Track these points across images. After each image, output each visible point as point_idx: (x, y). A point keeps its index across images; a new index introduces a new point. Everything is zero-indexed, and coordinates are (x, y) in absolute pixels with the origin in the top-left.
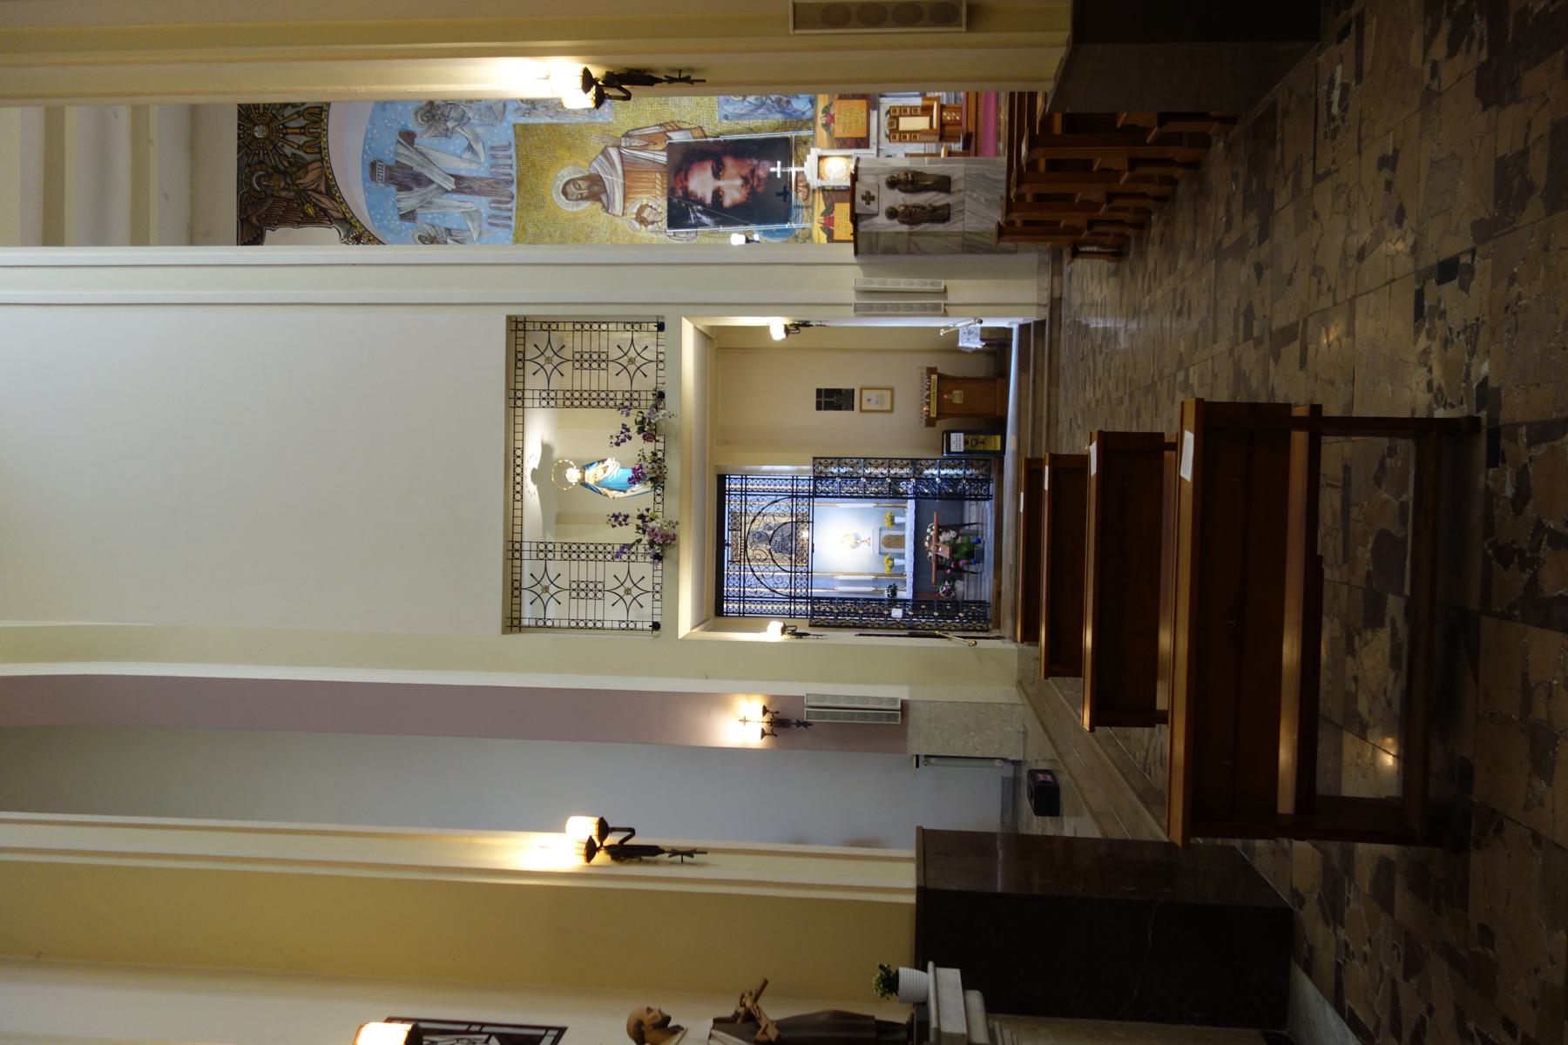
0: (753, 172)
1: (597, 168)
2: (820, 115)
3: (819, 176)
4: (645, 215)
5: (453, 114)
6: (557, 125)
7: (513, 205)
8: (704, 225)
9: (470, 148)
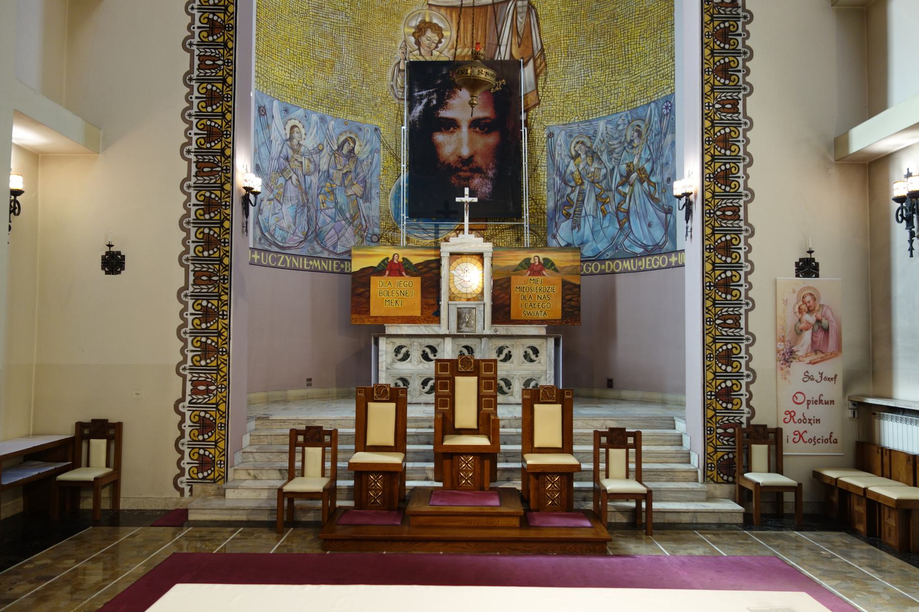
0: (478, 170)
2: (542, 256)
3: (454, 255)
4: (429, 33)
8: (411, 109)
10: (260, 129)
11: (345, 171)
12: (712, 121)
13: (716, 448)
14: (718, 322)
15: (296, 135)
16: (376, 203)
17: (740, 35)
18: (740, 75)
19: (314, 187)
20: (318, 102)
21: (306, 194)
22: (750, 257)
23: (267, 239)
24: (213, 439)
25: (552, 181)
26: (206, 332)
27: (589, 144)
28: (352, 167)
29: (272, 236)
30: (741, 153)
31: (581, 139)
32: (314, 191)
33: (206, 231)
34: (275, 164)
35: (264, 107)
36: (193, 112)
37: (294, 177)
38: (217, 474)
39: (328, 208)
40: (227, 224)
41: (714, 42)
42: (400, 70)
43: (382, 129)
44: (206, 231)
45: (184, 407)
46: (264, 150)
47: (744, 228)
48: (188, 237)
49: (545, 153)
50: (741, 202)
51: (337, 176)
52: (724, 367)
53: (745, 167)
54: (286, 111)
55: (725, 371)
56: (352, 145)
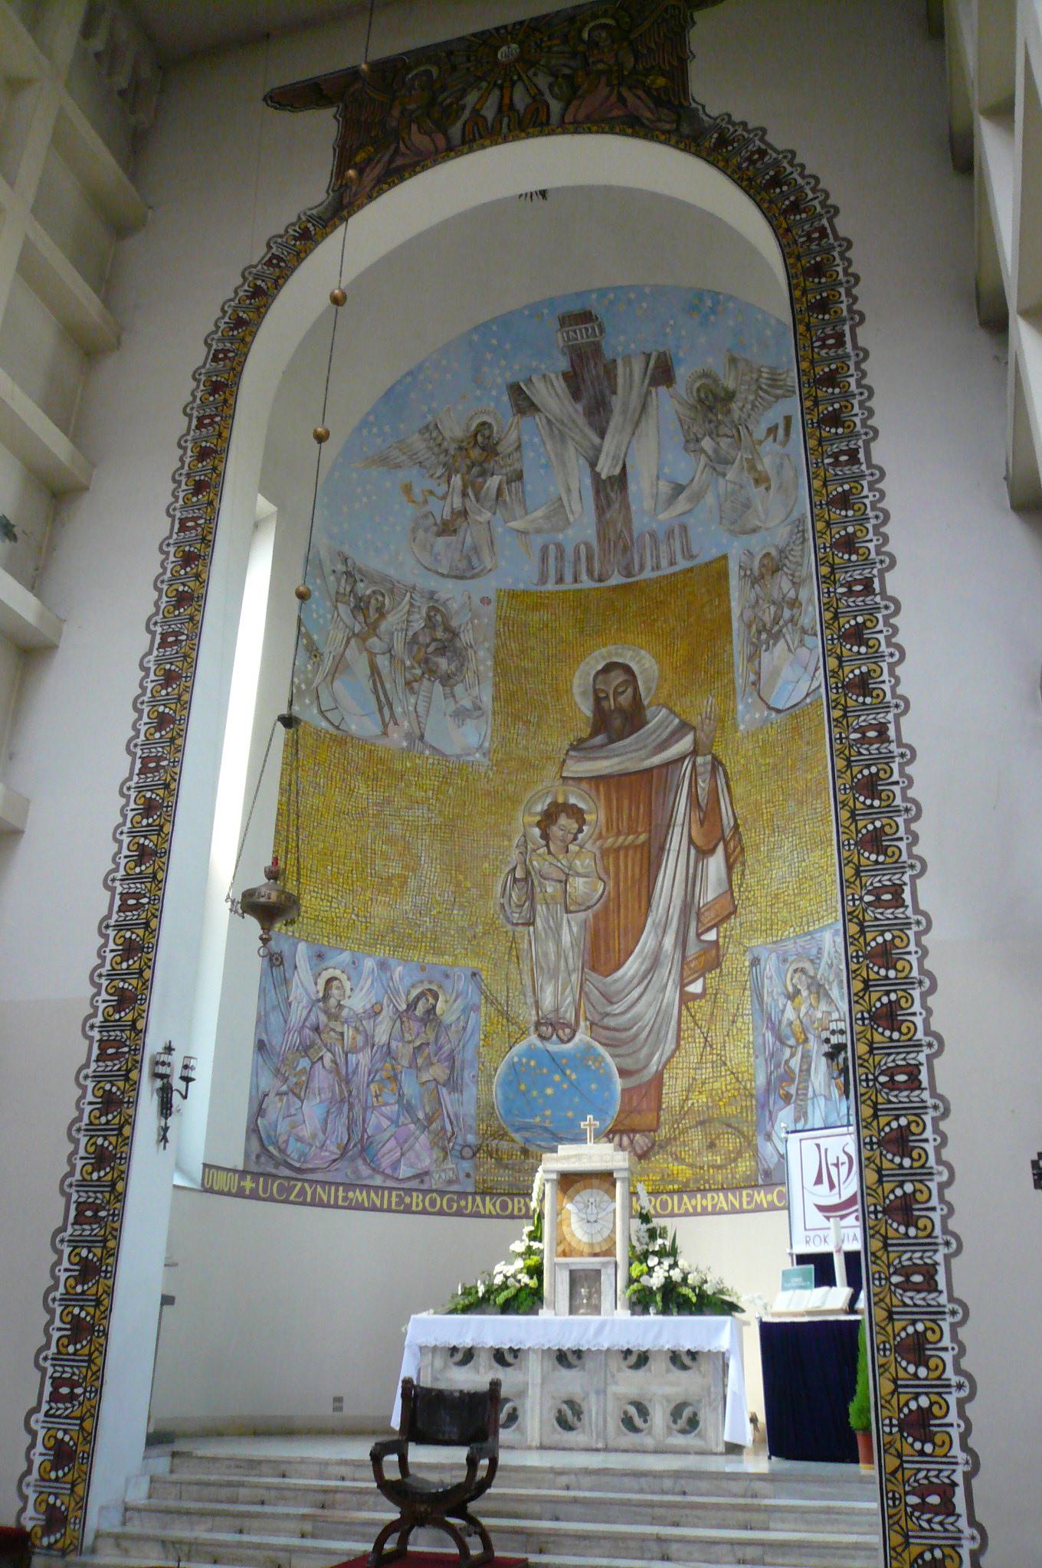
1: (658, 718)
4: (563, 820)
5: (724, 443)
6: (729, 632)
7: (586, 583)
9: (679, 489)
10: (269, 986)
11: (418, 1043)
12: (861, 924)
13: (907, 1537)
14: (895, 1279)
15: (335, 992)
16: (470, 1092)
17: (897, 783)
18: (902, 845)
19: (363, 1070)
20: (378, 939)
21: (348, 1082)
22: (946, 1154)
23: (271, 1156)
24: (69, 1478)
25: (760, 1040)
26: (80, 1299)
27: (812, 973)
28: (432, 1037)
29: (280, 1150)
30: (915, 973)
31: (801, 965)
32: (363, 1076)
33: (100, 1141)
34: (294, 1038)
35: (280, 954)
36: (104, 971)
37: (328, 1057)
38: (68, 1542)
39: (386, 1104)
40: (126, 1131)
41: (855, 799)
42: (515, 880)
43: (484, 975)
44: (100, 1141)
45: (38, 1422)
46: (275, 1019)
47: (930, 1102)
48: (75, 1152)
49: (747, 993)
50: (922, 1058)
51: (404, 1052)
52: (911, 1369)
53: (924, 996)
54: (320, 956)
55: (916, 1376)
56: (431, 1000)
